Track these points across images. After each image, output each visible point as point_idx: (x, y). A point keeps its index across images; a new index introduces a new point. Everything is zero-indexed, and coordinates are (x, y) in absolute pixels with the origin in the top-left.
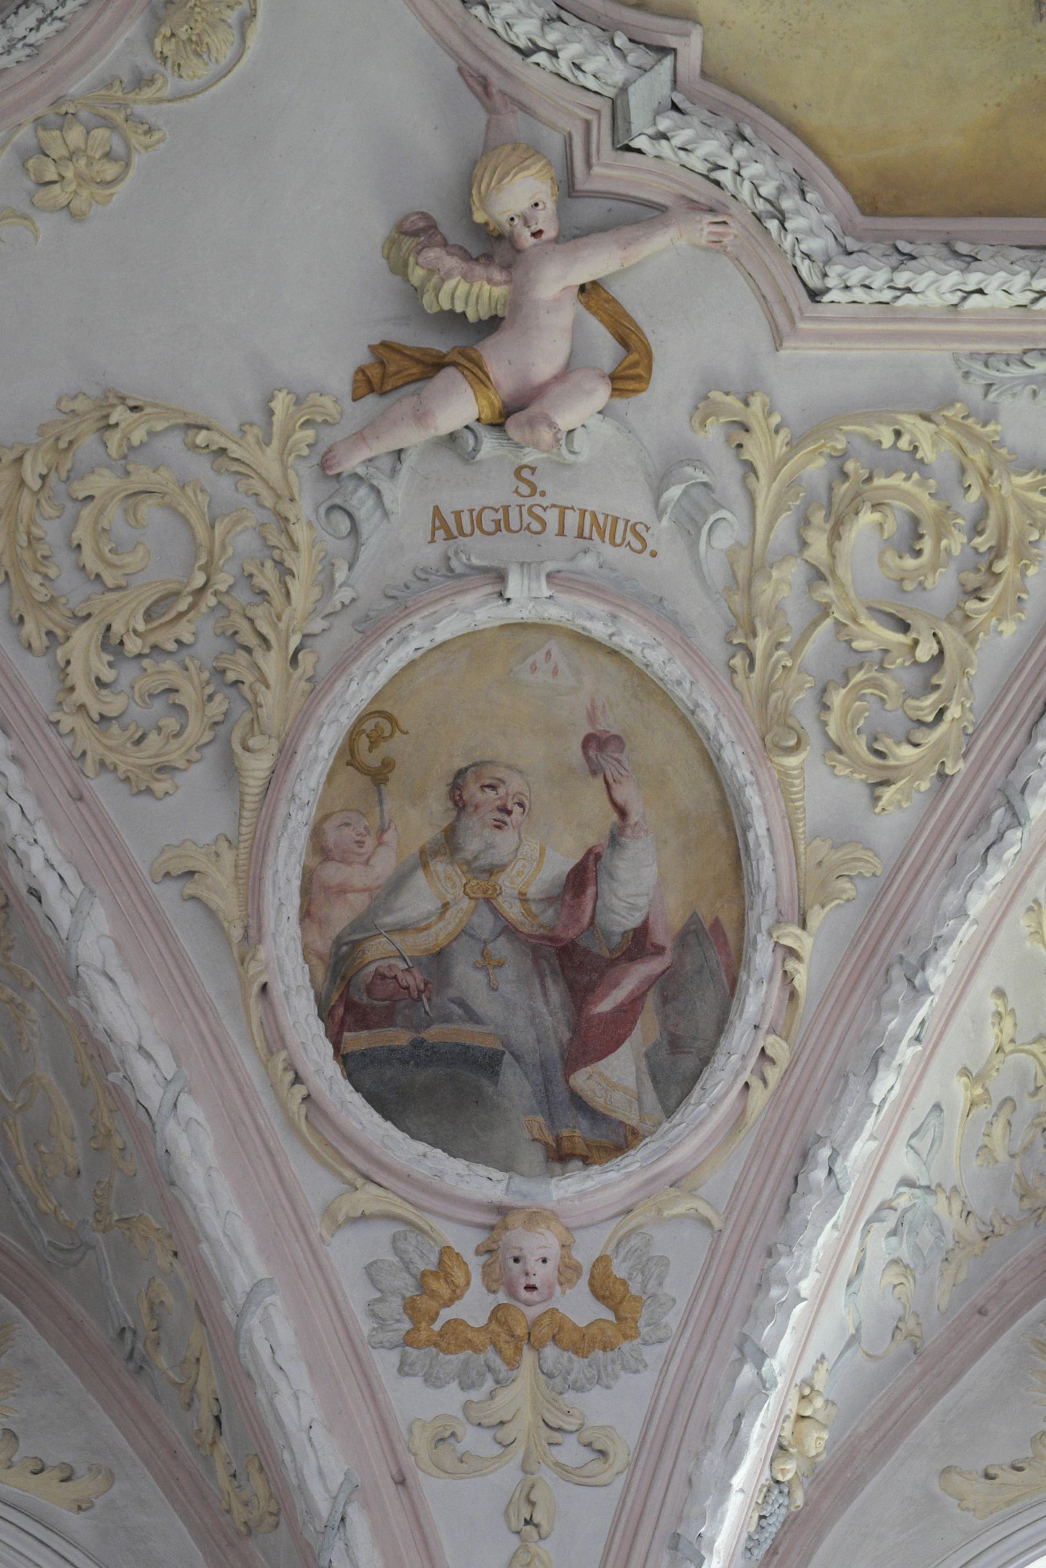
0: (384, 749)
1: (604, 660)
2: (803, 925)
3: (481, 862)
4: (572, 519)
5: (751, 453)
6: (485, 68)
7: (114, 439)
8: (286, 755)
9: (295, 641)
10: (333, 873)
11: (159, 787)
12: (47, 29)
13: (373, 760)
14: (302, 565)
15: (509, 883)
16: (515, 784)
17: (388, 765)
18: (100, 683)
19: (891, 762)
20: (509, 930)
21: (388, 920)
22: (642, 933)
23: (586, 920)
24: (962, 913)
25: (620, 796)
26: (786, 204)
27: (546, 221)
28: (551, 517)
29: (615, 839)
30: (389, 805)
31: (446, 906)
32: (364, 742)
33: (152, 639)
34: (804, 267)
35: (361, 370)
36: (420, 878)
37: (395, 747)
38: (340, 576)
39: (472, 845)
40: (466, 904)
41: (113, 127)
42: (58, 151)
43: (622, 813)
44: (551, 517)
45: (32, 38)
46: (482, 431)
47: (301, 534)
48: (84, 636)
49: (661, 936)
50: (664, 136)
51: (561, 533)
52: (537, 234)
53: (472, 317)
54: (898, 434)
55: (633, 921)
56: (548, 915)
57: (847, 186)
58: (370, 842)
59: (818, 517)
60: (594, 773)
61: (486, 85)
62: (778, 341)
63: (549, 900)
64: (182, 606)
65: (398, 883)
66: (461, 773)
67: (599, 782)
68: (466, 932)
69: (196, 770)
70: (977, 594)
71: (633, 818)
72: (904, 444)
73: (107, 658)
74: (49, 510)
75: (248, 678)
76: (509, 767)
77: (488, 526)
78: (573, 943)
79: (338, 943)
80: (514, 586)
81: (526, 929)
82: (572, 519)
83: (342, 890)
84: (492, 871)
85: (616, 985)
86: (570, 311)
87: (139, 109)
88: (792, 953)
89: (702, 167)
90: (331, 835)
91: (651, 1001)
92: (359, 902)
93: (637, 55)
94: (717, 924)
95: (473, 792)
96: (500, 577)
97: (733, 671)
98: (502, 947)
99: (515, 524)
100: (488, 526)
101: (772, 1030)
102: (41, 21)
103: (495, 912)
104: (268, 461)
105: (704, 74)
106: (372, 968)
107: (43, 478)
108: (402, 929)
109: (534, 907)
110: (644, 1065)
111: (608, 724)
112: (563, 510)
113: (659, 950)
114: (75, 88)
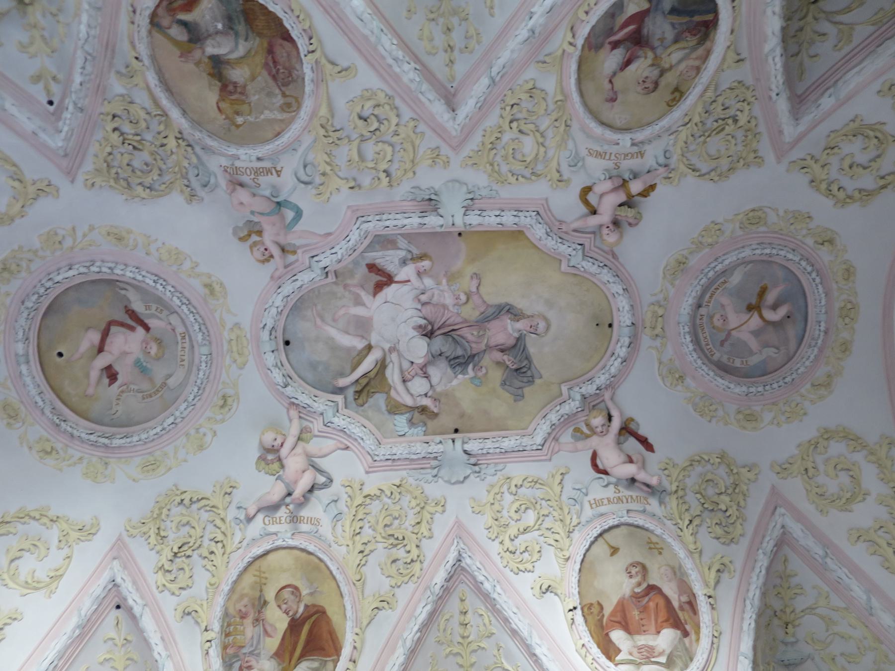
0: (671, 97)
1: (605, 120)
2: (564, 51)
3: (654, 67)
4: (607, 157)
5: (558, 175)
6: (613, 260)
7: (718, 172)
8: (702, 96)
9: (689, 125)
10: (697, 63)
11: (736, 84)
12: (713, 265)
13: (677, 94)
14: (681, 144)
15: (649, 61)
16: (639, 89)
17: (673, 93)
18: (741, 111)
19: (529, 95)
20: (653, 49)
21: (687, 51)
22: (613, 48)
23: (629, 52)
24: (512, 51)
25: (610, 86)
26: (546, 235)
27: (605, 231)
28: (613, 157)
29: (614, 74)
30: (675, 82)
31: (669, 55)
32: (677, 99)
33: (724, 122)
34: (541, 220)
35: (653, 191)
36: (674, 62)
37: (669, 97)
38: (672, 142)
39: (656, 72)
40: (663, 56)
41: (701, 243)
42: (715, 237)
43: (610, 81)
44: (613, 157)
45: (716, 263)
46: (628, 179)
47: (679, 152)
48: (741, 123)
49: (608, 47)
50: (574, 249)
51: (611, 154)
52: (608, 227)
53: (626, 207)
54: (517, 179)
55: (616, 51)
56: (641, 53)
57: (528, 239)
58: (685, 72)
59: (541, 159)
60: (616, 92)
61: (613, 257)
62: (547, 200)
63: (638, 57)
64: (715, 132)
65: (680, 61)
66: (653, 91)
67: (615, 89)
68: (666, 48)
69: (723, 89)
70: (497, 138)
71: (607, 80)
72: (516, 177)
73: (737, 118)
74: (739, 153)
75: (703, 115)
76: (639, 93)
77: (630, 155)
78: (635, 45)
79: (703, 44)
80: (629, 143)
81: (648, 49)
82: (607, 157)
83: (697, 58)
84: (653, 65)
85: (626, 33)
86: (601, 210)
87: (694, 246)
88: (571, 44)
89: (565, 242)
90: (694, 73)
91: (617, 28)
92: (694, 55)
93: (579, 266)
94: (590, 49)
95: (651, 86)
96: (633, 144)
97: (571, 120)
98: (656, 43)
99: (623, 156)
100: (630, 155)
101: (583, 21)
102: (715, 267)
103: (655, 53)
104: (682, 168)
105: (561, 260)
106: (697, 37)
107: (738, 162)
108: (684, 48)
109: (643, 55)
110: (625, 9)
111: (609, 105)
112: (609, 159)
113: (610, 43)
114: (707, 250)
